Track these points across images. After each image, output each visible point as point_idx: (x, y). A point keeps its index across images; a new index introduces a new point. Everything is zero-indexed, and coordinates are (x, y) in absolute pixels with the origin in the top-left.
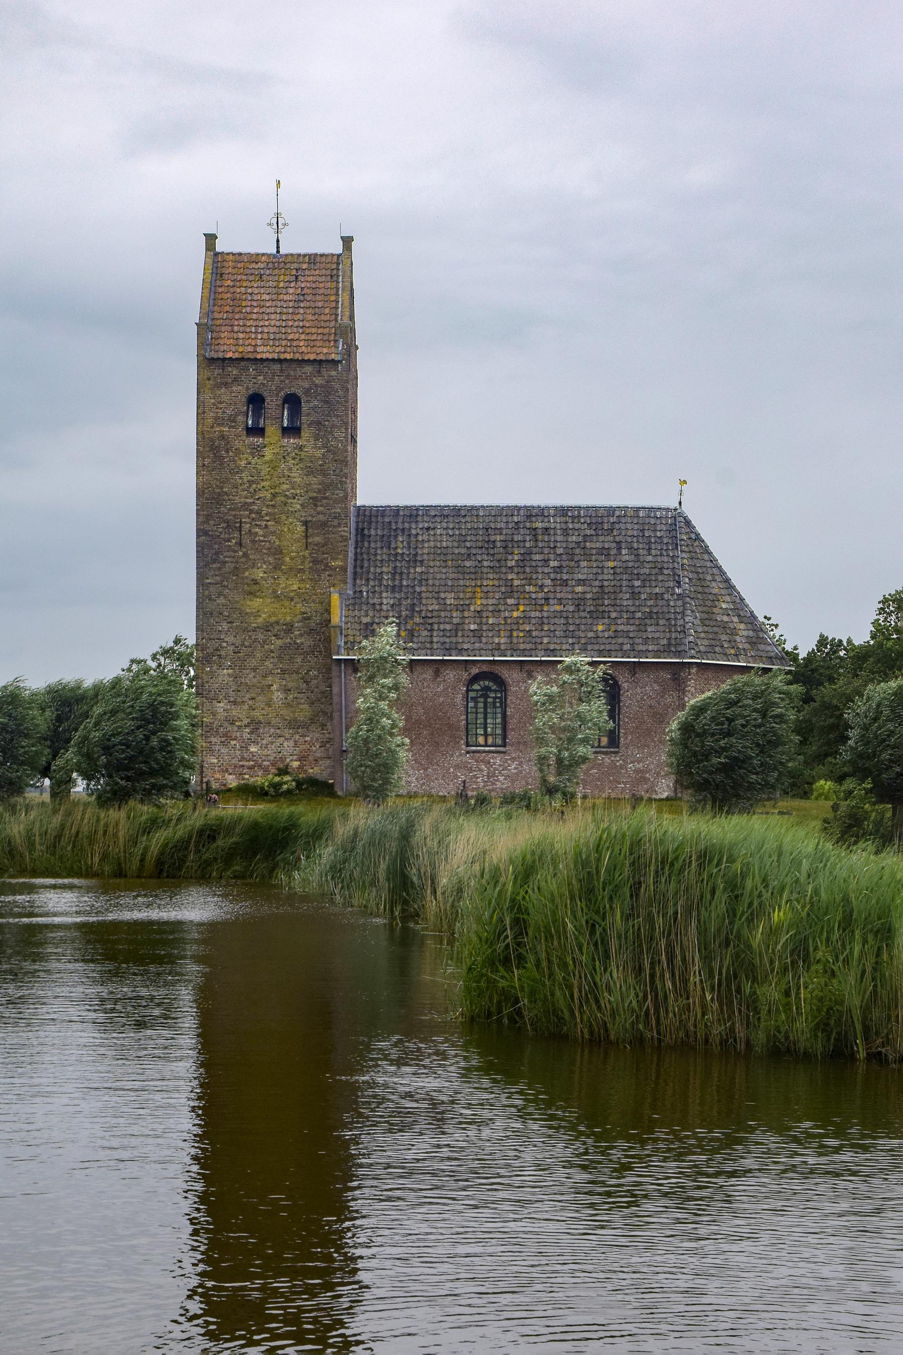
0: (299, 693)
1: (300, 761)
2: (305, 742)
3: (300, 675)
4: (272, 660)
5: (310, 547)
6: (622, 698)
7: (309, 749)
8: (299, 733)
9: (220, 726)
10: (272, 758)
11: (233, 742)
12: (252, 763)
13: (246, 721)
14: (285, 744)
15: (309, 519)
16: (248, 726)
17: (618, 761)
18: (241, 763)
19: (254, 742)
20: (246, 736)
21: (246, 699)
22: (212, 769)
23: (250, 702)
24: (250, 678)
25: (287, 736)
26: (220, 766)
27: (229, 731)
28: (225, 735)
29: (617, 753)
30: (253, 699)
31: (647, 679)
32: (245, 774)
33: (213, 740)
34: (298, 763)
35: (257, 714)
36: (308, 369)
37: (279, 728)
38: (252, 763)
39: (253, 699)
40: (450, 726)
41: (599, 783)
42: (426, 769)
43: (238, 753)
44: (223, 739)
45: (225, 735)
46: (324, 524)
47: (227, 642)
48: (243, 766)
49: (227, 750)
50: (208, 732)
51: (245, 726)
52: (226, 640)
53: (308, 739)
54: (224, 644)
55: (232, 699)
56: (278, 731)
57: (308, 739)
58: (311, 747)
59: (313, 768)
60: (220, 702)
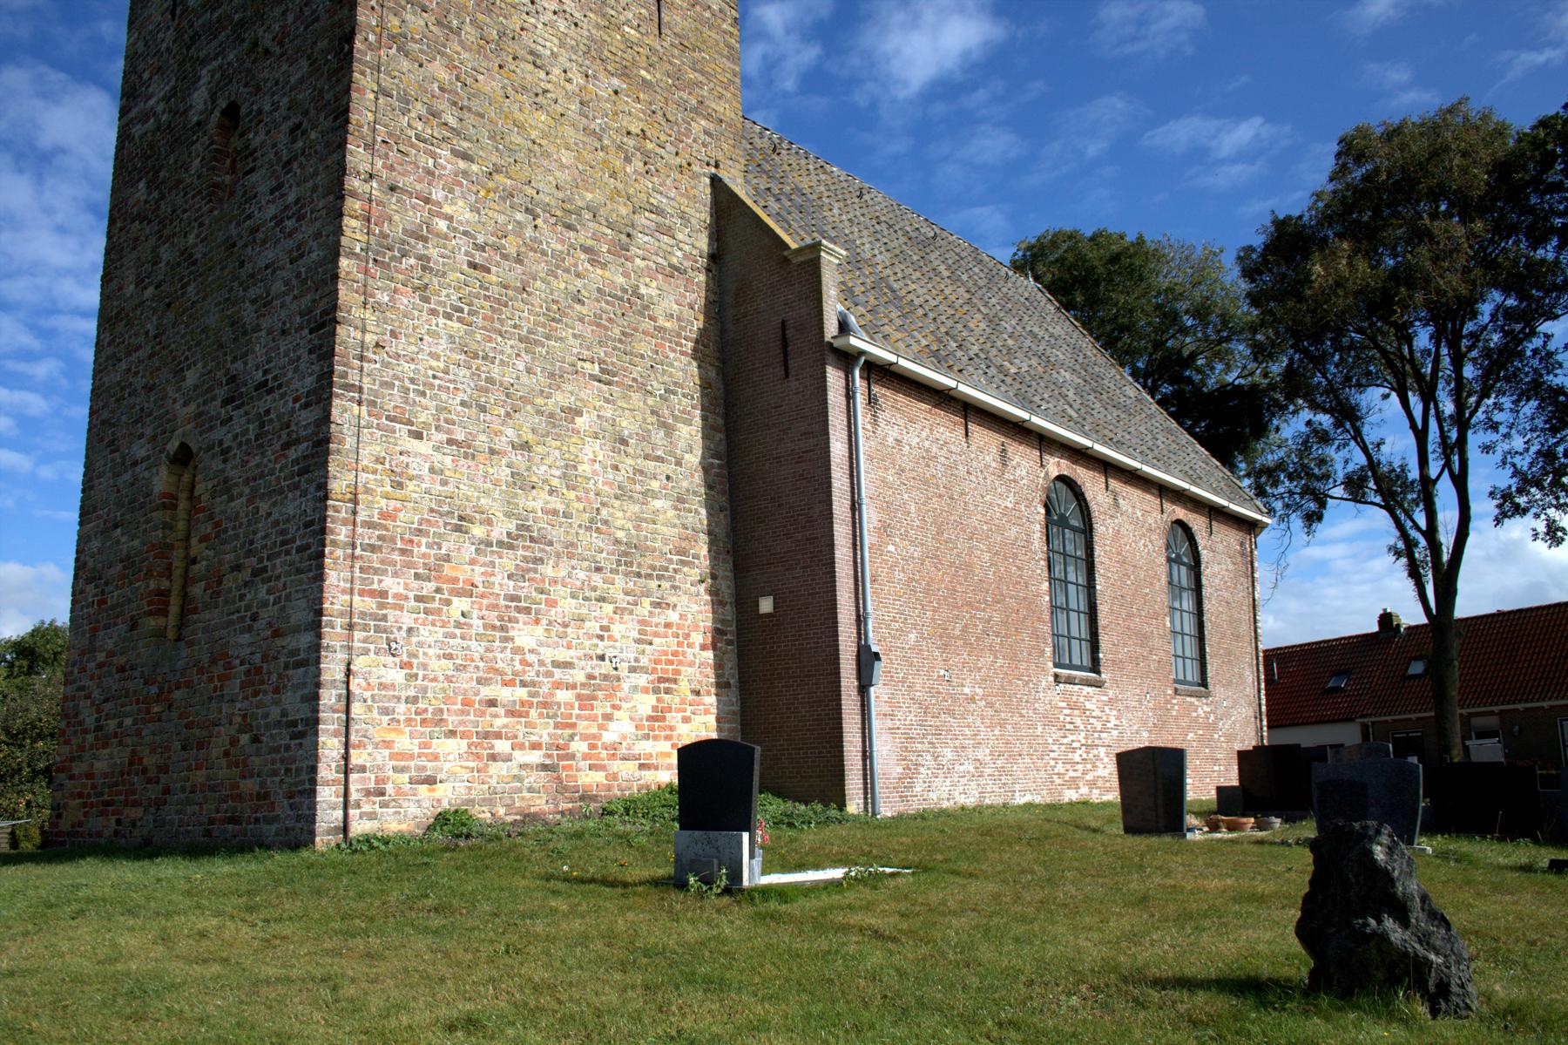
0: (647, 457)
1: (656, 691)
2: (668, 625)
3: (650, 401)
4: (578, 326)
7: (675, 654)
8: (648, 594)
9: (419, 532)
10: (579, 676)
11: (460, 604)
12: (522, 693)
13: (503, 528)
14: (617, 629)
16: (511, 547)
18: (487, 692)
19: (527, 611)
20: (502, 584)
21: (502, 443)
22: (385, 711)
23: (518, 458)
24: (513, 368)
25: (623, 600)
26: (415, 700)
27: (447, 559)
28: (432, 571)
30: (526, 446)
32: (498, 736)
33: (391, 584)
34: (651, 699)
35: (537, 502)
37: (598, 569)
38: (522, 693)
39: (526, 446)
42: (1002, 726)
43: (477, 648)
44: (429, 587)
45: (432, 571)
47: (450, 218)
48: (492, 703)
49: (439, 633)
50: (373, 548)
51: (500, 543)
52: (447, 209)
53: (673, 616)
54: (442, 225)
55: (460, 436)
56: (597, 579)
57: (673, 616)
58: (680, 644)
59: (686, 720)
60: (418, 436)
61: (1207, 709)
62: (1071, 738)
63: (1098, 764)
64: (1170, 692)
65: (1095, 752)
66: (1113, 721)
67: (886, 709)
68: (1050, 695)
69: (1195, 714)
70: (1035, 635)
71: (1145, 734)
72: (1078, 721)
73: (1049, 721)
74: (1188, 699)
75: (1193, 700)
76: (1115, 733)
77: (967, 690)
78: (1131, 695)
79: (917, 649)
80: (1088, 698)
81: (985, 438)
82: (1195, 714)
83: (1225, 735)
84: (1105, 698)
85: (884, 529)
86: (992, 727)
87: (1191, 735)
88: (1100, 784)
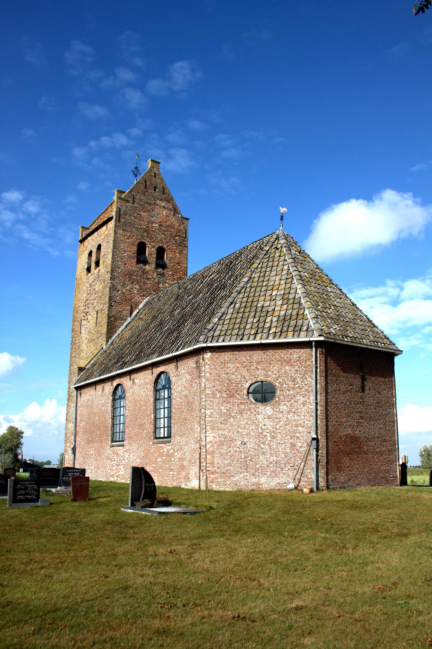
5: (98, 324)
6: (172, 392)
15: (99, 309)
17: (170, 449)
29: (169, 442)
31: (183, 371)
36: (104, 228)
40: (106, 427)
41: (161, 470)
46: (102, 310)
61: (168, 448)
62: (113, 463)
63: (120, 470)
64: (151, 443)
65: (119, 467)
66: (127, 456)
67: (78, 458)
68: (109, 451)
69: (162, 451)
70: (107, 435)
71: (139, 460)
72: (115, 458)
73: (108, 458)
74: (160, 445)
75: (162, 445)
76: (127, 461)
77: (91, 453)
78: (135, 447)
79: (83, 445)
80: (120, 450)
81: (99, 387)
82: (162, 451)
83: (179, 459)
84: (125, 450)
85: (80, 421)
86: (95, 461)
87: (160, 459)
88: (120, 476)
